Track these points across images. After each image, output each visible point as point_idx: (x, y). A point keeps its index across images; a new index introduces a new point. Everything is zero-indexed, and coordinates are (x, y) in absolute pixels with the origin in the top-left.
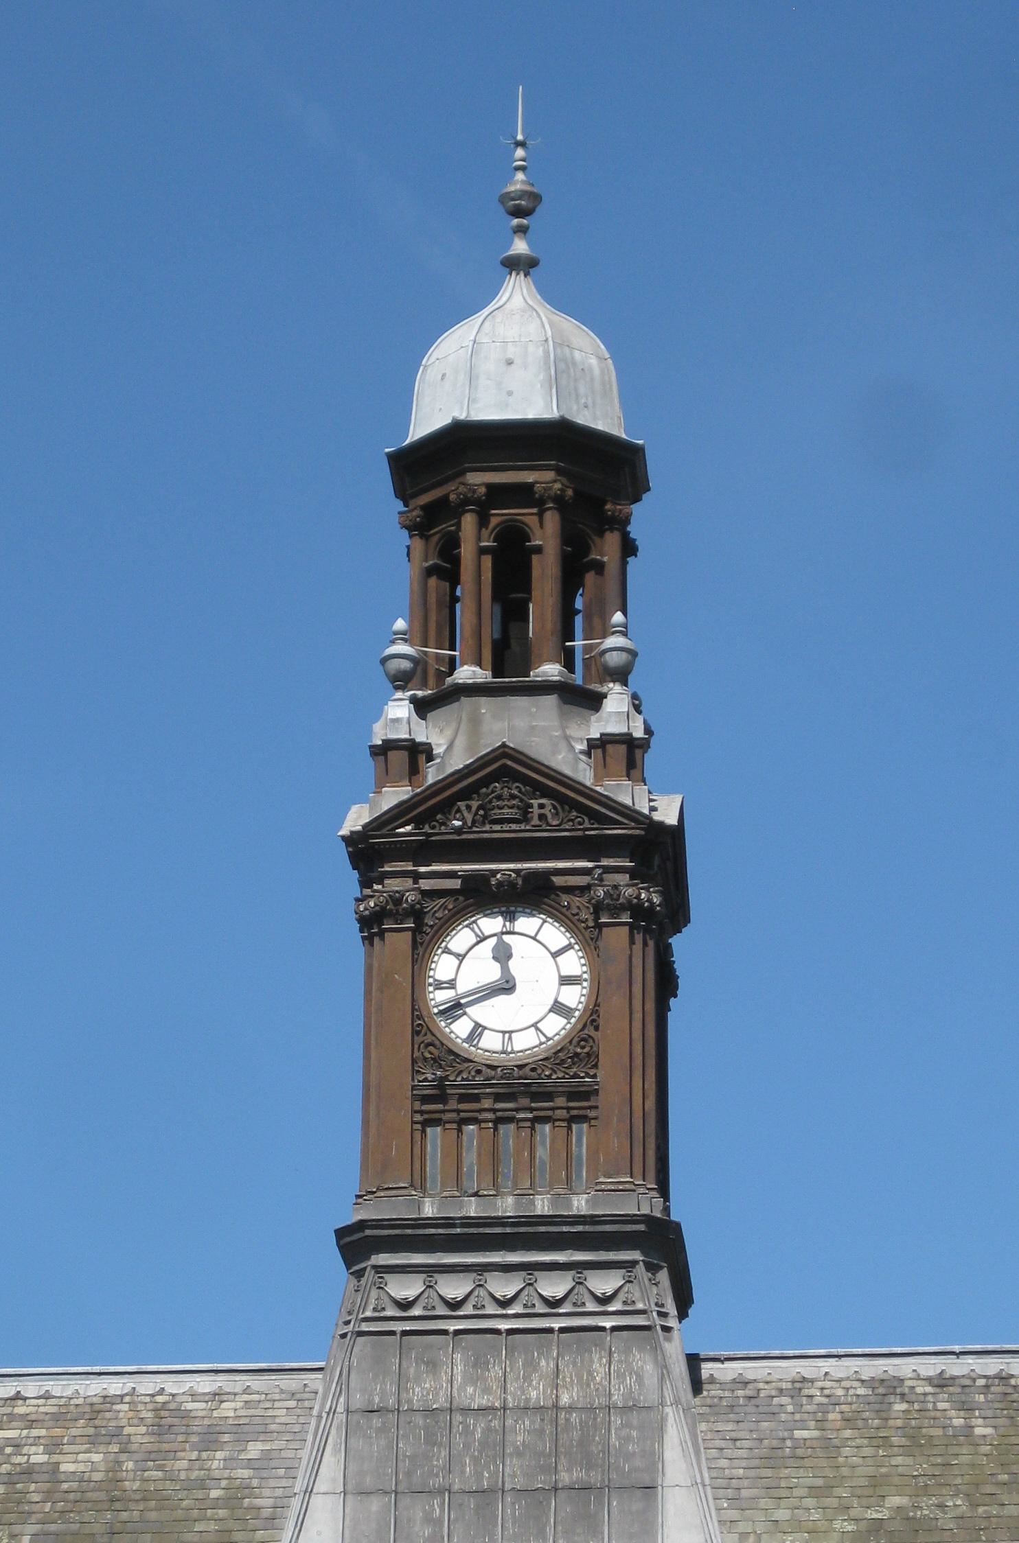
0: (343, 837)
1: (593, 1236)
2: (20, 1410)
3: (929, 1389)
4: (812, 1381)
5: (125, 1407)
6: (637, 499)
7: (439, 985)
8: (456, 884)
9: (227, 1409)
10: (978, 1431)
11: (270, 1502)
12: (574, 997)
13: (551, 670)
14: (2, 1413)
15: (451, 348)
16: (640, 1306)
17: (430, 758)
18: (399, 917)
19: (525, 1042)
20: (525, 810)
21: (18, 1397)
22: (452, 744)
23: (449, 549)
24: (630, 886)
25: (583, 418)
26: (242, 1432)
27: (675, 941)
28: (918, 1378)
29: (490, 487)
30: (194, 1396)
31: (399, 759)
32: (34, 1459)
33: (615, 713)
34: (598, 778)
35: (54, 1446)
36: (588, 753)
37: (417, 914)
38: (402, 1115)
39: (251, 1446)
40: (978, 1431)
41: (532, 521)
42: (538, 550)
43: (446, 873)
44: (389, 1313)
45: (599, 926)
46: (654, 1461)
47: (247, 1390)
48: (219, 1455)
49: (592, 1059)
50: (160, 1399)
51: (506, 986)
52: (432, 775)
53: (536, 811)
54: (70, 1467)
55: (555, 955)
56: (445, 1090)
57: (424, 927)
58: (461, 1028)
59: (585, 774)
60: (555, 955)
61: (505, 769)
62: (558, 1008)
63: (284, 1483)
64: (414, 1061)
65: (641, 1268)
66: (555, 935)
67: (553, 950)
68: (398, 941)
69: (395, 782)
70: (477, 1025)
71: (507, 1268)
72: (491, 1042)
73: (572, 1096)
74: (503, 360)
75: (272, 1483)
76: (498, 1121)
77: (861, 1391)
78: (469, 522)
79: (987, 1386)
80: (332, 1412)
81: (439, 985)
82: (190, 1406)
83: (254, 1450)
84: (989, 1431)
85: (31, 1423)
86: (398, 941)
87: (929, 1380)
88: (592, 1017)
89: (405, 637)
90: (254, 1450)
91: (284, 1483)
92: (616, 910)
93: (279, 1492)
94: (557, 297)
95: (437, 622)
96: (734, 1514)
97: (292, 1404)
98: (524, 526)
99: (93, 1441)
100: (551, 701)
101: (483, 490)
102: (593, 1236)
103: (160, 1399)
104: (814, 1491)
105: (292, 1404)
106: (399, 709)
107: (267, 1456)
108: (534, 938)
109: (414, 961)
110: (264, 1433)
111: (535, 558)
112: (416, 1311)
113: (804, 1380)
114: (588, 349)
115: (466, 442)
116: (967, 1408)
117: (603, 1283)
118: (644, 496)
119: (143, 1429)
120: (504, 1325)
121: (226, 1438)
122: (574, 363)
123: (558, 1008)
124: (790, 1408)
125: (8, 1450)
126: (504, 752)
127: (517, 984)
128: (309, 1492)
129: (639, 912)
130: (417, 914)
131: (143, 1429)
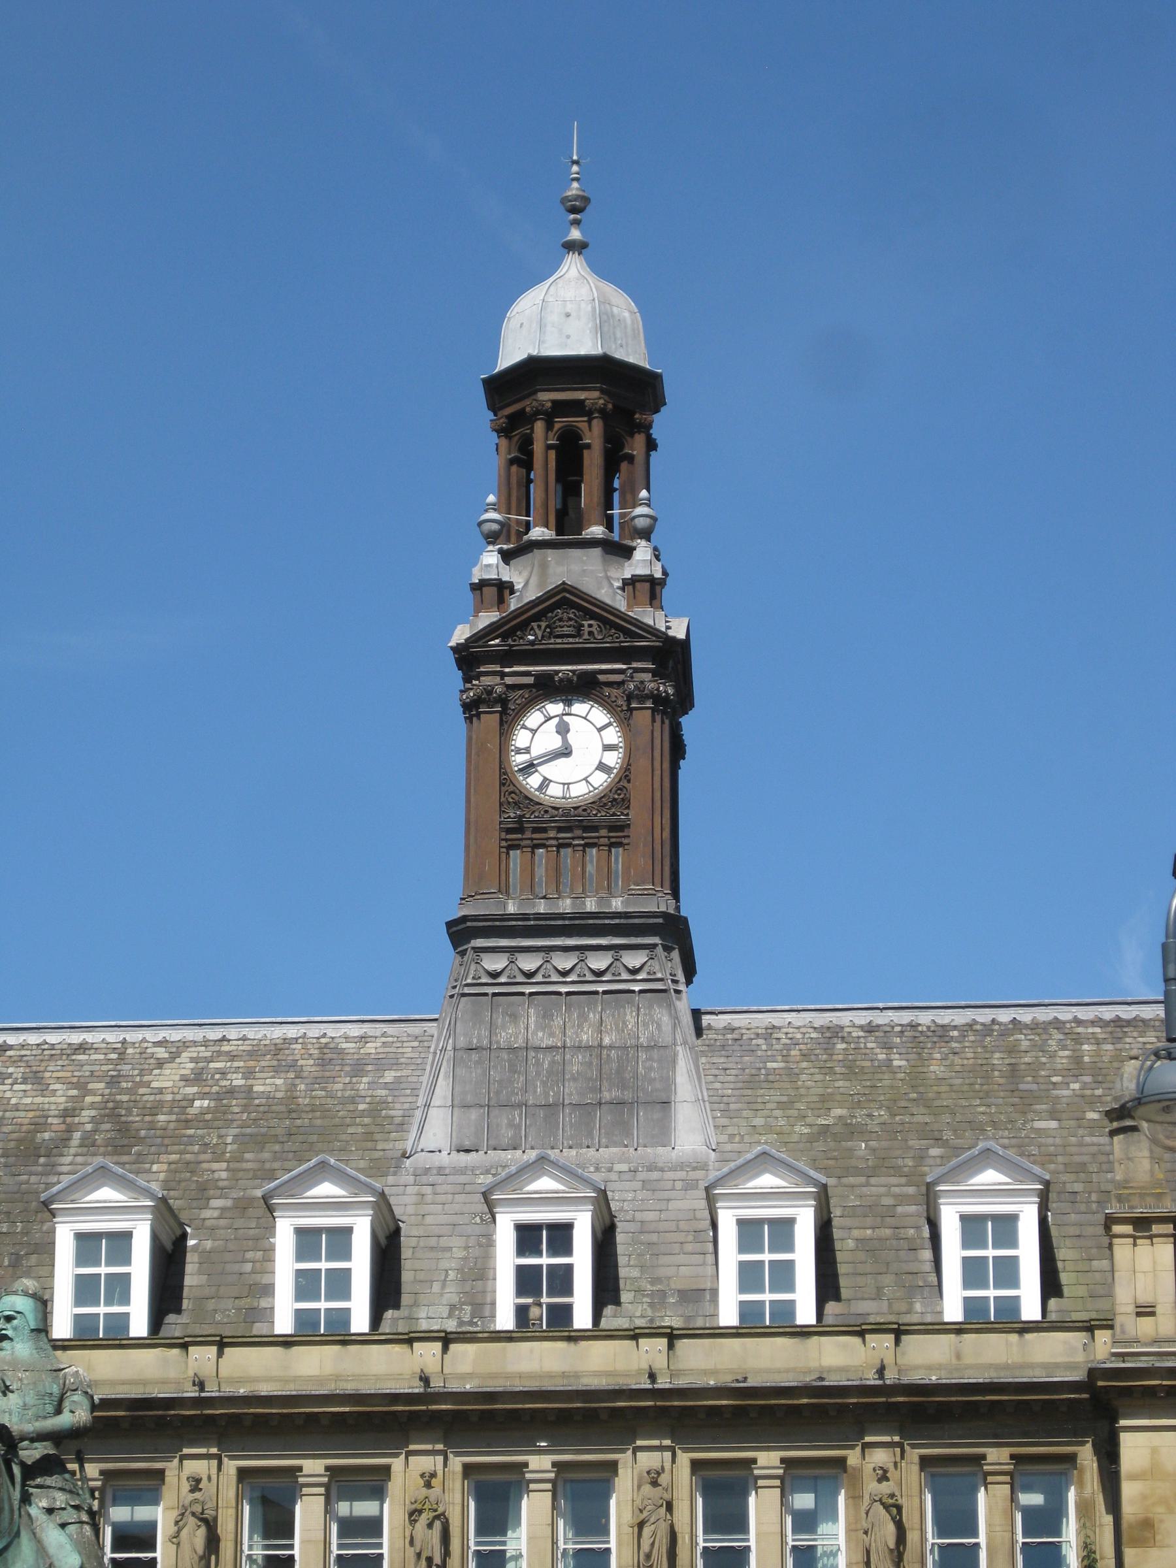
0: (452, 648)
1: (626, 927)
2: (226, 1048)
3: (861, 1034)
4: (780, 1028)
5: (299, 1046)
6: (657, 411)
7: (519, 751)
9: (370, 1048)
10: (896, 1063)
11: (400, 1113)
12: (613, 759)
13: (596, 531)
14: (1, 1049)
15: (526, 305)
16: (659, 975)
17: (512, 592)
18: (490, 703)
19: (579, 791)
20: (579, 628)
21: (224, 1039)
22: (527, 582)
23: (526, 446)
24: (655, 681)
25: (619, 354)
26: (381, 1064)
27: (684, 720)
28: (854, 1026)
29: (554, 402)
30: (347, 1038)
31: (490, 593)
32: (235, 1083)
33: (642, 560)
34: (629, 606)
35: (249, 1074)
36: (623, 589)
37: (503, 701)
38: (493, 842)
39: (387, 1073)
41: (584, 426)
42: (588, 446)
43: (524, 672)
44: (483, 980)
45: (631, 710)
46: (669, 1084)
47: (384, 1035)
48: (365, 1080)
49: (625, 803)
50: (323, 1040)
51: (565, 752)
52: (513, 604)
53: (586, 629)
54: (261, 1089)
55: (600, 730)
56: (523, 824)
57: (507, 710)
58: (534, 781)
59: (620, 603)
60: (600, 730)
61: (565, 600)
62: (602, 767)
63: (410, 1099)
64: (501, 804)
65: (660, 949)
66: (599, 716)
68: (490, 720)
69: (487, 609)
70: (545, 779)
72: (555, 791)
73: (612, 828)
74: (563, 314)
75: (402, 1099)
76: (559, 846)
77: (814, 1035)
78: (539, 427)
79: (902, 1032)
80: (444, 1049)
81: (519, 751)
82: (344, 1046)
83: (389, 1076)
84: (903, 1063)
85: (233, 1057)
86: (490, 720)
87: (861, 1027)
88: (626, 773)
89: (495, 507)
90: (389, 1076)
91: (410, 1099)
92: (642, 698)
93: (406, 1106)
94: (600, 269)
95: (517, 496)
96: (724, 1121)
97: (416, 1044)
98: (579, 431)
99: (277, 1070)
100: (597, 552)
101: (549, 404)
102: (626, 927)
103: (323, 1040)
104: (781, 1105)
105: (416, 1044)
106: (491, 557)
107: (398, 1081)
109: (501, 735)
110: (396, 1064)
111: (586, 452)
112: (503, 979)
113: (774, 1027)
114: (623, 306)
115: (537, 371)
116: (888, 1047)
117: (634, 960)
119: (312, 1062)
120: (564, 989)
121: (369, 1068)
122: (613, 316)
123: (602, 767)
124: (764, 1047)
125: (217, 1076)
126: (564, 588)
127: (573, 750)
128: (427, 1106)
129: (657, 698)
130: (503, 701)
131: (312, 1062)
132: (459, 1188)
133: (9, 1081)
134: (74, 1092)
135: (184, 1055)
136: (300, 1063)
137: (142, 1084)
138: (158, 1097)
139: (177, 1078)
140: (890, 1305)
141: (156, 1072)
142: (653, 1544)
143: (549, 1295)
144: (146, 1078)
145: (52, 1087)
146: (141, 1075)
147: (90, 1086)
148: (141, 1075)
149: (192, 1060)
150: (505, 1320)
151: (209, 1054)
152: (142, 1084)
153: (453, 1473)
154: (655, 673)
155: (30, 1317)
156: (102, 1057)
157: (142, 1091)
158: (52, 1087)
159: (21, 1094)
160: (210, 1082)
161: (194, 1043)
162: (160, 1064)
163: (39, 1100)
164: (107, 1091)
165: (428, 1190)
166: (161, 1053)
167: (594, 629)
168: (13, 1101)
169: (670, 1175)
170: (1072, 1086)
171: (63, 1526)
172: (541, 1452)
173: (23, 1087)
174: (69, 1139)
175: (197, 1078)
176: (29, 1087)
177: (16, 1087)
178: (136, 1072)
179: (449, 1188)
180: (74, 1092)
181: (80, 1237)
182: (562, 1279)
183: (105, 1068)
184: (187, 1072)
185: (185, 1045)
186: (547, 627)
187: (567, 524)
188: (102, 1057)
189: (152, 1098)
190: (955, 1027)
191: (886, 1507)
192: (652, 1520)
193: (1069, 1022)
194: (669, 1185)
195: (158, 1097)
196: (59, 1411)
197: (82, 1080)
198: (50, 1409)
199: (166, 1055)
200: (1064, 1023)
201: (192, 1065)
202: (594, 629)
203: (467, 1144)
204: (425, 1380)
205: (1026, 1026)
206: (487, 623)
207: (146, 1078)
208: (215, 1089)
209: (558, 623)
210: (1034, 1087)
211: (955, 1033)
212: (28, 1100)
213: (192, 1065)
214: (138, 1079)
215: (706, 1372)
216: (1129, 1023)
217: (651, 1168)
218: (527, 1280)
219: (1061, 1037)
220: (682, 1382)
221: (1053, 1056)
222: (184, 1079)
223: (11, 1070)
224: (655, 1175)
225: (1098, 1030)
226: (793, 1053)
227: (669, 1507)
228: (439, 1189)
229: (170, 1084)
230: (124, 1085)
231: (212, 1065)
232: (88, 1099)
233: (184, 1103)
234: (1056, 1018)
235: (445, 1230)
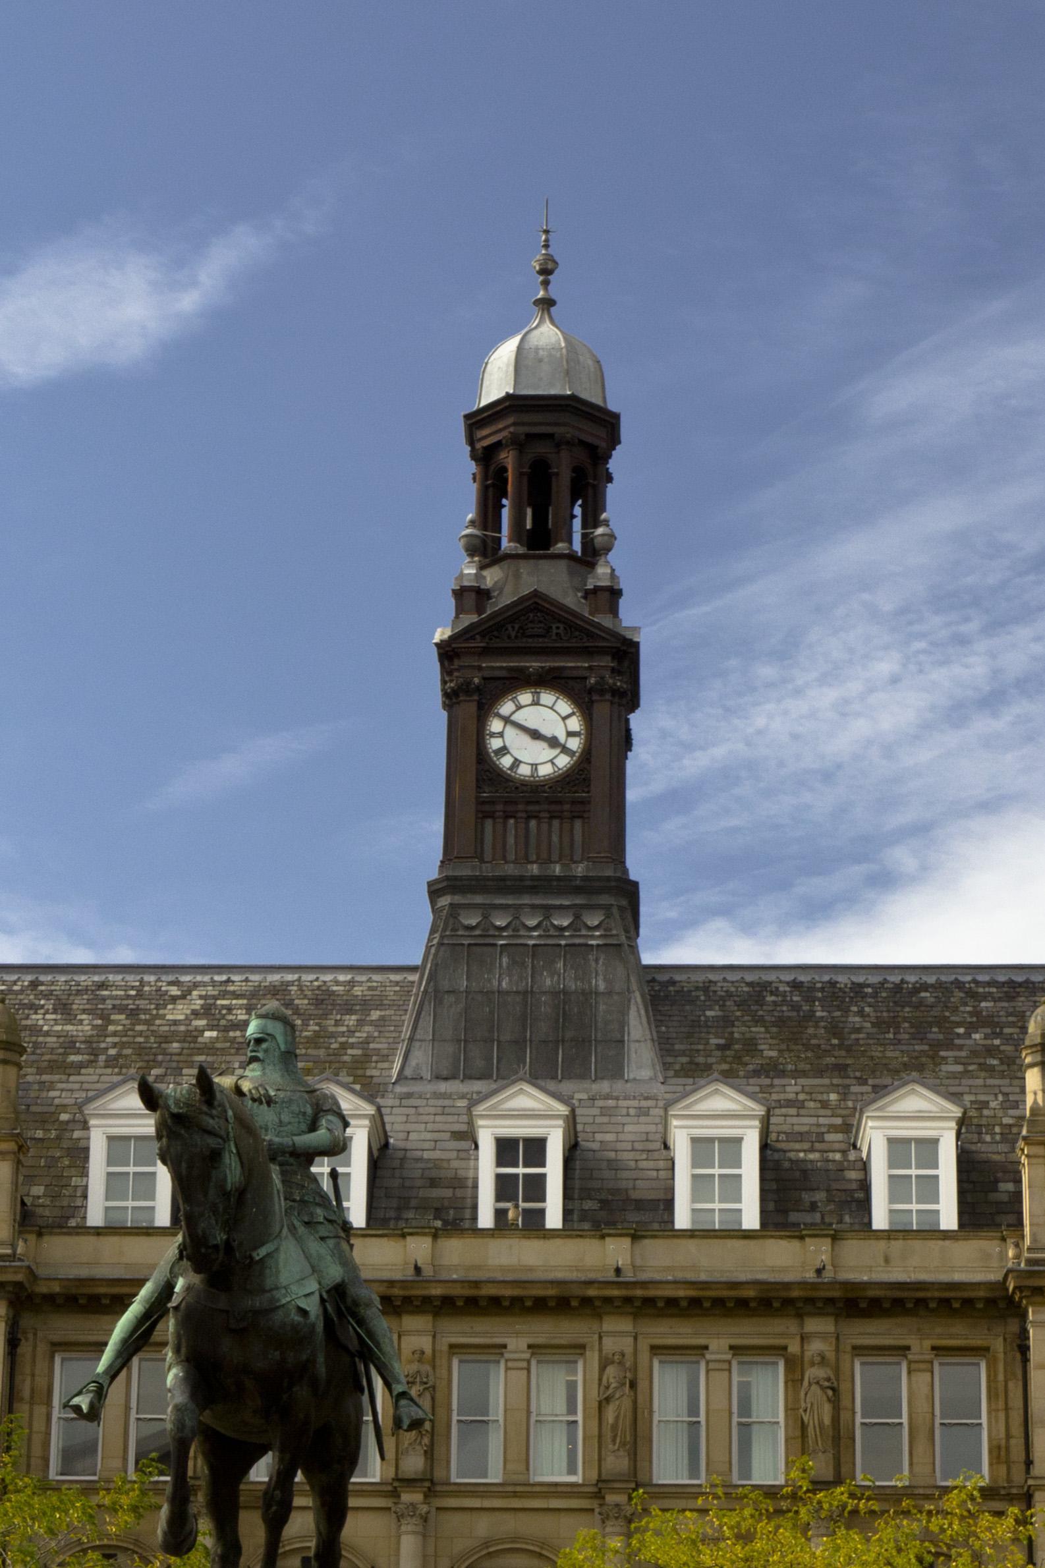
0: (436, 644)
2: (232, 988)
3: (788, 989)
4: (715, 983)
5: (295, 988)
7: (493, 735)
8: (503, 674)
9: (358, 991)
10: (819, 1014)
11: (386, 1046)
16: (614, 932)
17: (489, 598)
18: (468, 692)
19: (545, 771)
21: (228, 981)
25: (584, 395)
26: (366, 1005)
27: (631, 716)
28: (781, 982)
30: (337, 983)
31: (470, 599)
32: (240, 1017)
36: (585, 598)
39: (372, 1012)
40: (819, 1014)
42: (557, 474)
44: (460, 933)
45: (592, 702)
46: (623, 1024)
48: (354, 1017)
50: (316, 983)
53: (555, 631)
60: (564, 719)
61: (535, 607)
63: (394, 1035)
64: (477, 780)
65: (615, 910)
67: (564, 715)
68: (469, 708)
69: (467, 613)
70: (516, 760)
71: (533, 907)
72: (524, 770)
75: (387, 1035)
77: (746, 989)
79: (823, 988)
81: (493, 735)
82: (335, 988)
83: (375, 1015)
84: (824, 1014)
86: (469, 708)
87: (788, 983)
88: (586, 758)
90: (375, 1015)
91: (394, 1035)
92: (602, 692)
93: (391, 1040)
96: (670, 1060)
97: (398, 988)
100: (563, 565)
101: (523, 437)
102: (586, 887)
103: (316, 983)
104: (719, 1047)
105: (398, 988)
107: (382, 1018)
108: (551, 708)
109: (478, 720)
110: (380, 1006)
111: (554, 479)
112: (477, 932)
113: (710, 982)
116: (811, 1000)
118: (618, 447)
119: (306, 1002)
121: (358, 1007)
122: (579, 362)
124: (702, 998)
125: (224, 1012)
126: (535, 594)
129: (616, 692)
131: (306, 1002)
132: (439, 1110)
133: (42, 1011)
134: (100, 1022)
135: (195, 993)
136: (296, 1002)
137: (158, 1016)
138: (173, 1028)
139: (189, 1012)
140: (823, 1218)
141: (170, 1007)
142: (617, 1418)
143: (524, 1201)
144: (161, 1012)
145: (79, 1017)
146: (157, 1009)
147: (113, 1017)
148: (157, 1009)
149: (201, 997)
150: (486, 1219)
151: (216, 993)
152: (158, 1016)
153: (441, 1351)
154: (613, 670)
155: (280, 1039)
156: (122, 993)
157: (158, 1022)
158: (79, 1017)
159: (52, 1023)
160: (218, 1016)
161: (204, 984)
162: (174, 999)
163: (69, 1027)
164: (128, 1022)
165: (413, 1111)
166: (174, 991)
167: (561, 631)
168: (45, 1028)
169: (622, 1103)
170: (974, 1036)
171: (322, 1239)
172: (517, 1334)
173: (53, 1016)
174: (96, 1061)
175: (207, 1011)
176: (59, 1017)
177: (48, 1017)
178: (153, 1006)
179: (432, 1110)
180: (100, 1022)
181: (111, 1139)
182: (536, 1186)
183: (125, 1002)
184: (198, 1007)
185: (196, 985)
186: (521, 628)
187: (539, 540)
188: (122, 993)
189: (167, 1028)
190: (868, 986)
191: (823, 1388)
192: (617, 1396)
193: (969, 983)
194: (624, 1112)
195: (173, 1028)
196: (313, 1127)
197: (106, 1012)
198: (304, 1127)
199: (179, 993)
200: (964, 983)
201: (201, 1002)
202: (561, 631)
203: (445, 1073)
204: (418, 1269)
205: (932, 986)
206: (466, 624)
207: (161, 1012)
208: (223, 1022)
209: (530, 625)
210: (941, 1037)
211: (870, 990)
212: (59, 1028)
213: (201, 1002)
214: (154, 1012)
215: (668, 1269)
216: (1020, 985)
217: (607, 1097)
218: (505, 1187)
219: (962, 995)
220: (644, 1276)
221: (955, 1010)
222: (195, 1013)
223: (42, 1002)
224: (611, 1103)
225: (994, 990)
226: (728, 1003)
227: (633, 1385)
228: (421, 1110)
229: (182, 1017)
230: (143, 1017)
231: (219, 1002)
232: (111, 1028)
233: (195, 1033)
234: (956, 979)
235: (427, 1145)
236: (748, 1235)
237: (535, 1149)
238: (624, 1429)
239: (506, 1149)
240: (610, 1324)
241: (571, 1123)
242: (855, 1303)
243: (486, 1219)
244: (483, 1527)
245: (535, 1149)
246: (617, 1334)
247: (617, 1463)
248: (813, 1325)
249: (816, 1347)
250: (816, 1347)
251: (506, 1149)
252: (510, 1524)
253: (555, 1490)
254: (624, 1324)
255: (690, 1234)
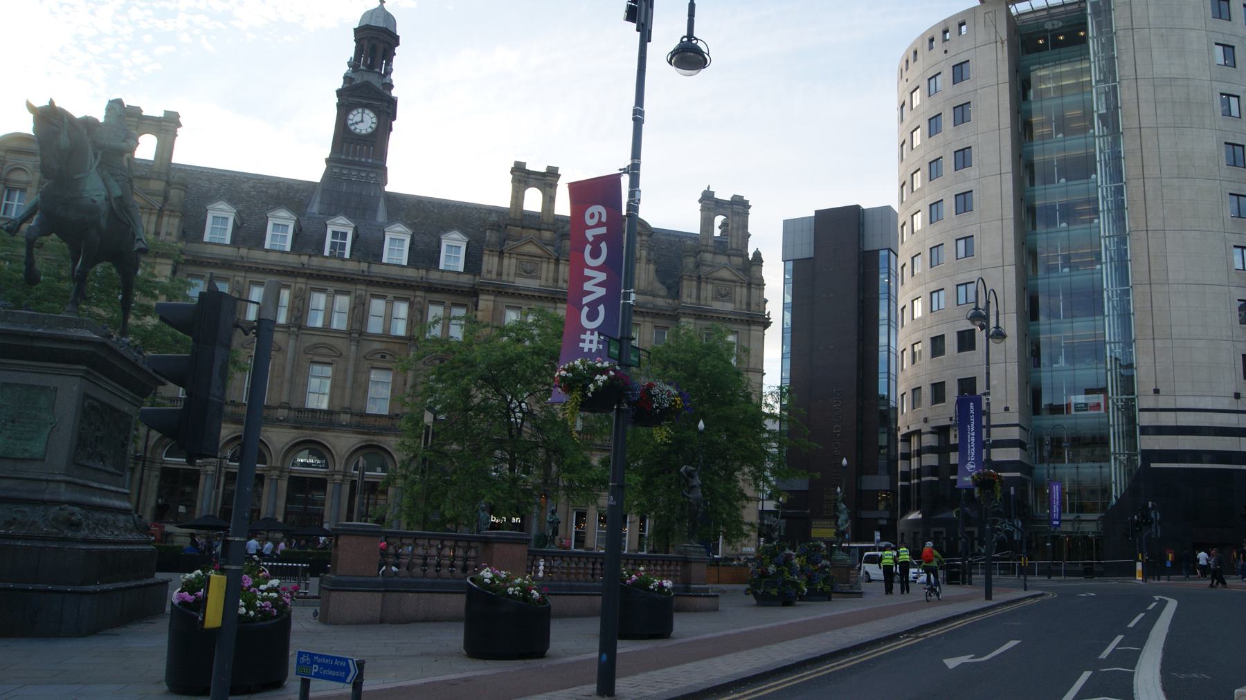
182: (343, 246)
218: (333, 245)
236: (403, 266)
237: (344, 235)
238: (359, 313)
239: (335, 234)
240: (359, 287)
241: (356, 229)
242: (431, 288)
243: (327, 253)
244: (315, 340)
245: (344, 235)
246: (361, 289)
247: (356, 326)
248: (418, 293)
249: (418, 299)
250: (418, 299)
251: (335, 234)
252: (323, 340)
253: (336, 331)
254: (364, 287)
255: (387, 264)
